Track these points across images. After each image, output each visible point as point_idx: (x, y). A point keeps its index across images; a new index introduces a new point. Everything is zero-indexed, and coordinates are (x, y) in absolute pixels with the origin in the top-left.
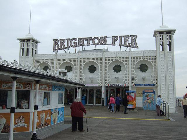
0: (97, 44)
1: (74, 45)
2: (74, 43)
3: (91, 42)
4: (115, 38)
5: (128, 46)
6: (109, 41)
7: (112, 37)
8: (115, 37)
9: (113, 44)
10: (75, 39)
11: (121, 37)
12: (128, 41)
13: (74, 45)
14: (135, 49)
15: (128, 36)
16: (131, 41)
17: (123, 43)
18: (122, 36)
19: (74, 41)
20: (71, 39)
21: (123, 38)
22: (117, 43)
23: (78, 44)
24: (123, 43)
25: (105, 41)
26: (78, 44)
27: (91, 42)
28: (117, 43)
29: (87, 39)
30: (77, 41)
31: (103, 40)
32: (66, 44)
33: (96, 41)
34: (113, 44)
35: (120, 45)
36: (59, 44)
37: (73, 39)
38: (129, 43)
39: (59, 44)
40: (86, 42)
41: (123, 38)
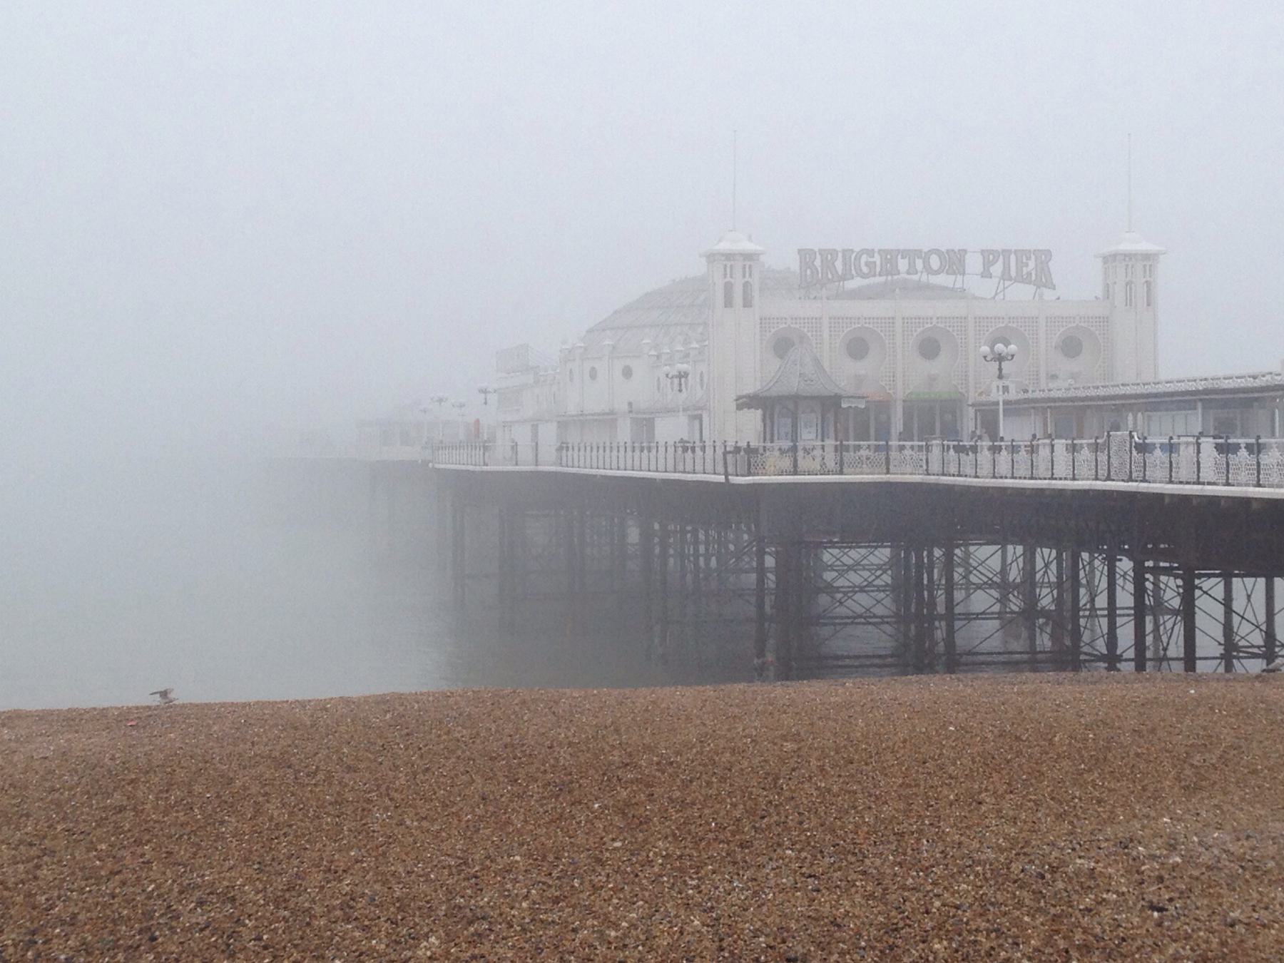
0: (936, 273)
1: (865, 270)
2: (866, 264)
3: (919, 264)
4: (989, 257)
5: (1026, 280)
6: (974, 263)
7: (982, 252)
8: (992, 252)
9: (986, 274)
10: (870, 253)
11: (1006, 253)
12: (1027, 265)
13: (865, 270)
14: (1048, 294)
15: (1027, 253)
16: (1033, 267)
17: (1013, 274)
18: (1009, 252)
19: (864, 258)
20: (857, 249)
21: (1013, 257)
22: (997, 269)
23: (878, 269)
24: (1013, 274)
25: (961, 261)
26: (878, 269)
27: (919, 264)
28: (997, 269)
29: (905, 253)
30: (877, 258)
31: (954, 261)
32: (839, 265)
33: (935, 262)
34: (986, 274)
35: (1006, 276)
36: (818, 263)
37: (863, 251)
38: (1029, 274)
39: (818, 263)
40: (903, 264)
41: (1013, 257)
